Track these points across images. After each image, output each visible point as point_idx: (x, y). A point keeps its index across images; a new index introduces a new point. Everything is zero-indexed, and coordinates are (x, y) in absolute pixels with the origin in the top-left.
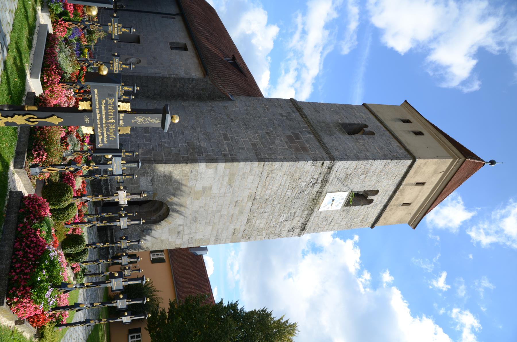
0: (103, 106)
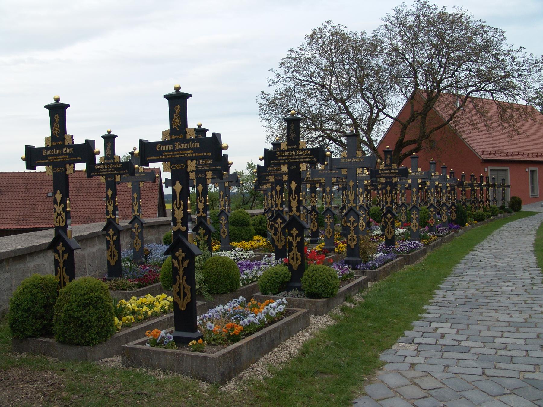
0: (282, 158)
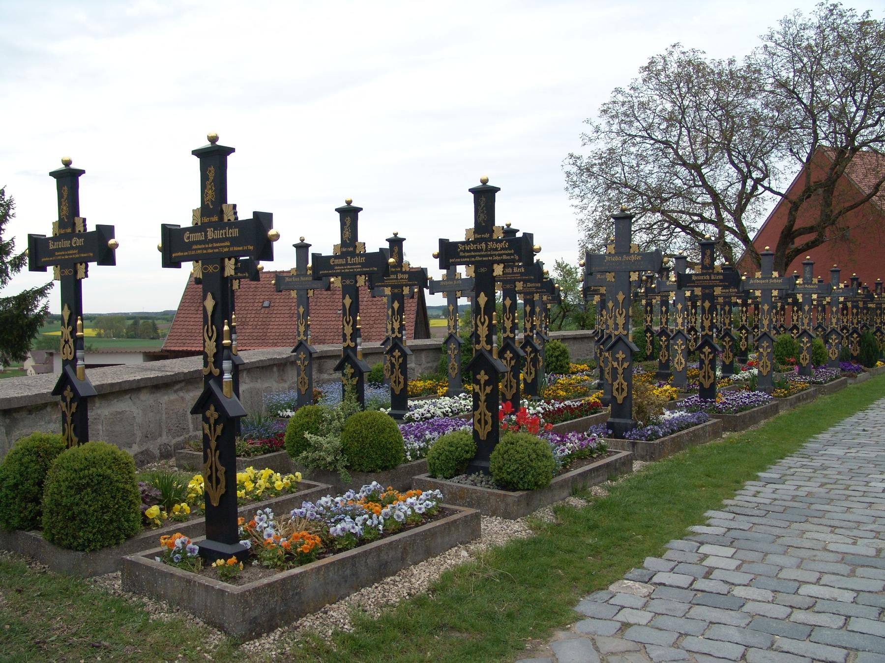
0: (467, 254)
